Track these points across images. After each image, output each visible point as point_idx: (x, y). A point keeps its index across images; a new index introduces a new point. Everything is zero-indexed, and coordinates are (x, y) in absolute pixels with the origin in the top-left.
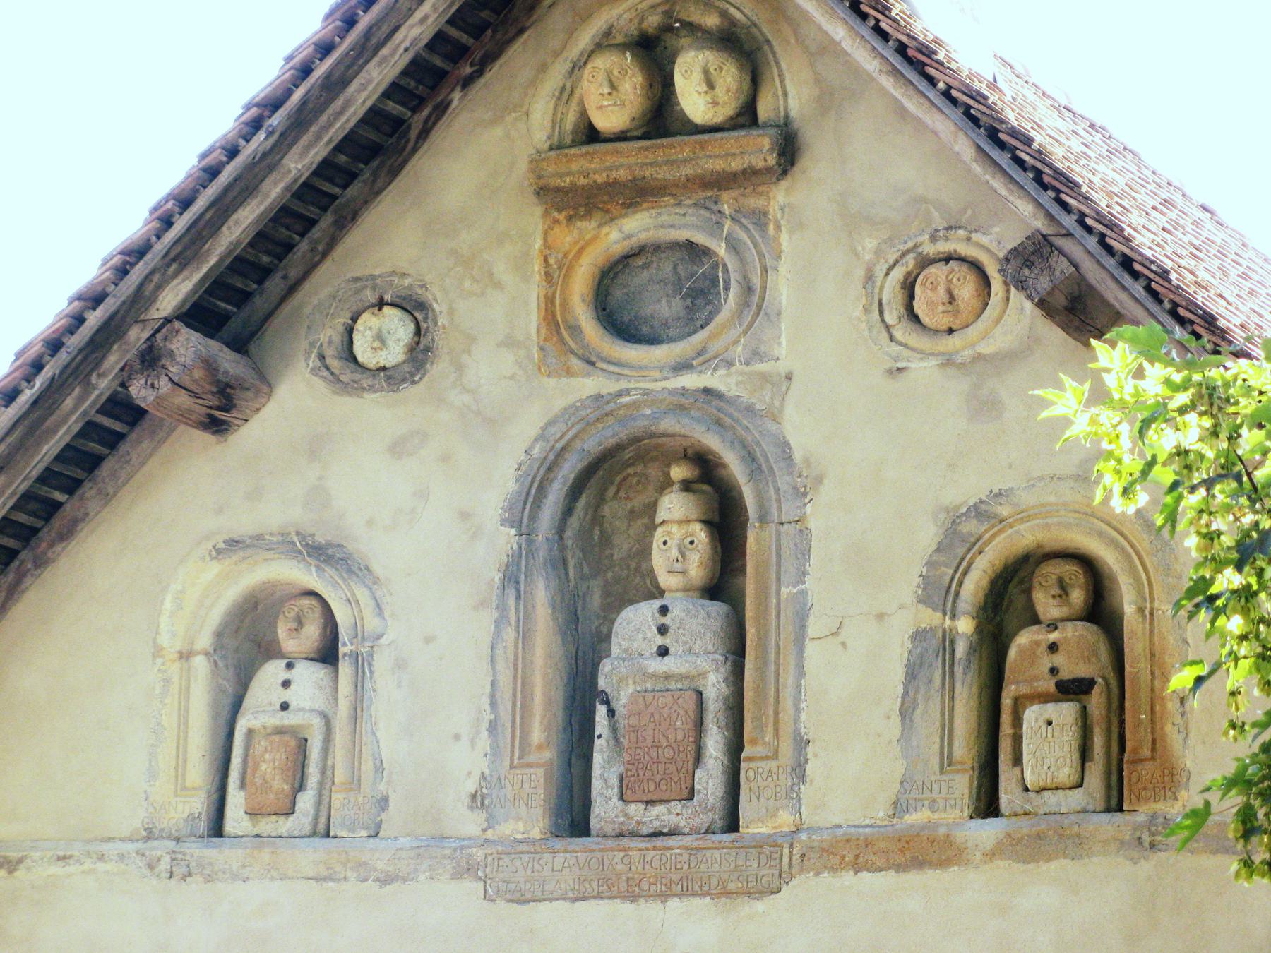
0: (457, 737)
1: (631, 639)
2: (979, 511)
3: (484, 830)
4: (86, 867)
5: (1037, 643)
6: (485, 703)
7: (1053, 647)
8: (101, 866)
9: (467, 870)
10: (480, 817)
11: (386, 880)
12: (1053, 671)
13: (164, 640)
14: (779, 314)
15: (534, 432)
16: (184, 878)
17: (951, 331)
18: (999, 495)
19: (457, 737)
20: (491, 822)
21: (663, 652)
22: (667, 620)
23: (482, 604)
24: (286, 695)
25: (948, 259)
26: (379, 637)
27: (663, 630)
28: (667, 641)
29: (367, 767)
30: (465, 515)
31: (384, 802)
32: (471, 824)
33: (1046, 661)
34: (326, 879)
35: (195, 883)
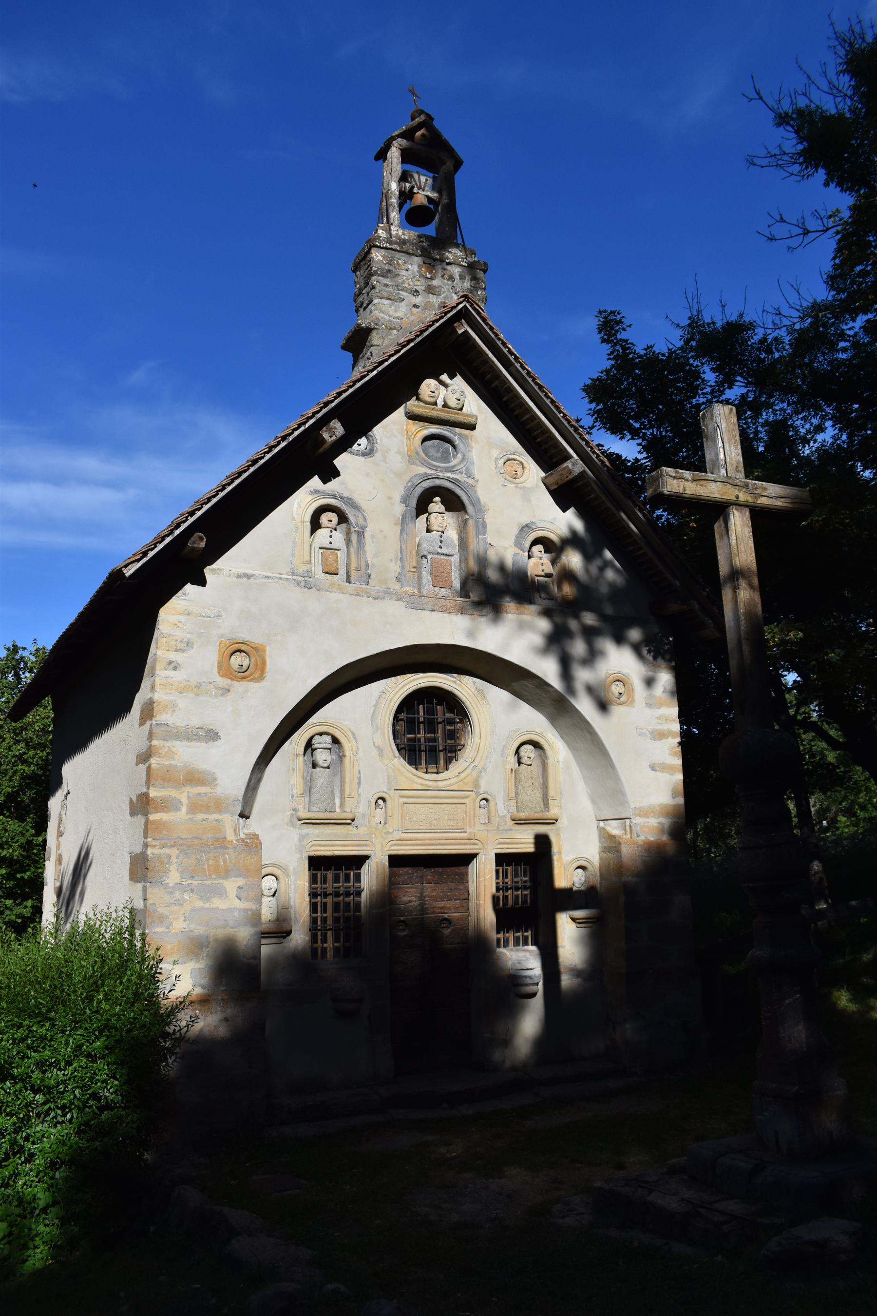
0: (391, 560)
1: (432, 542)
2: (527, 526)
3: (401, 588)
4: (275, 581)
5: (538, 562)
6: (399, 551)
7: (542, 564)
8: (280, 581)
9: (399, 599)
10: (399, 584)
11: (376, 598)
12: (543, 571)
13: (295, 516)
14: (474, 463)
15: (408, 479)
16: (309, 588)
17: (515, 478)
18: (532, 522)
19: (391, 560)
20: (402, 586)
21: (440, 547)
22: (442, 539)
23: (395, 524)
24: (330, 540)
25: (514, 460)
26: (366, 527)
27: (441, 542)
28: (441, 545)
29: (363, 565)
30: (390, 498)
31: (369, 575)
32: (397, 586)
33: (541, 568)
34: (357, 595)
35: (313, 591)
